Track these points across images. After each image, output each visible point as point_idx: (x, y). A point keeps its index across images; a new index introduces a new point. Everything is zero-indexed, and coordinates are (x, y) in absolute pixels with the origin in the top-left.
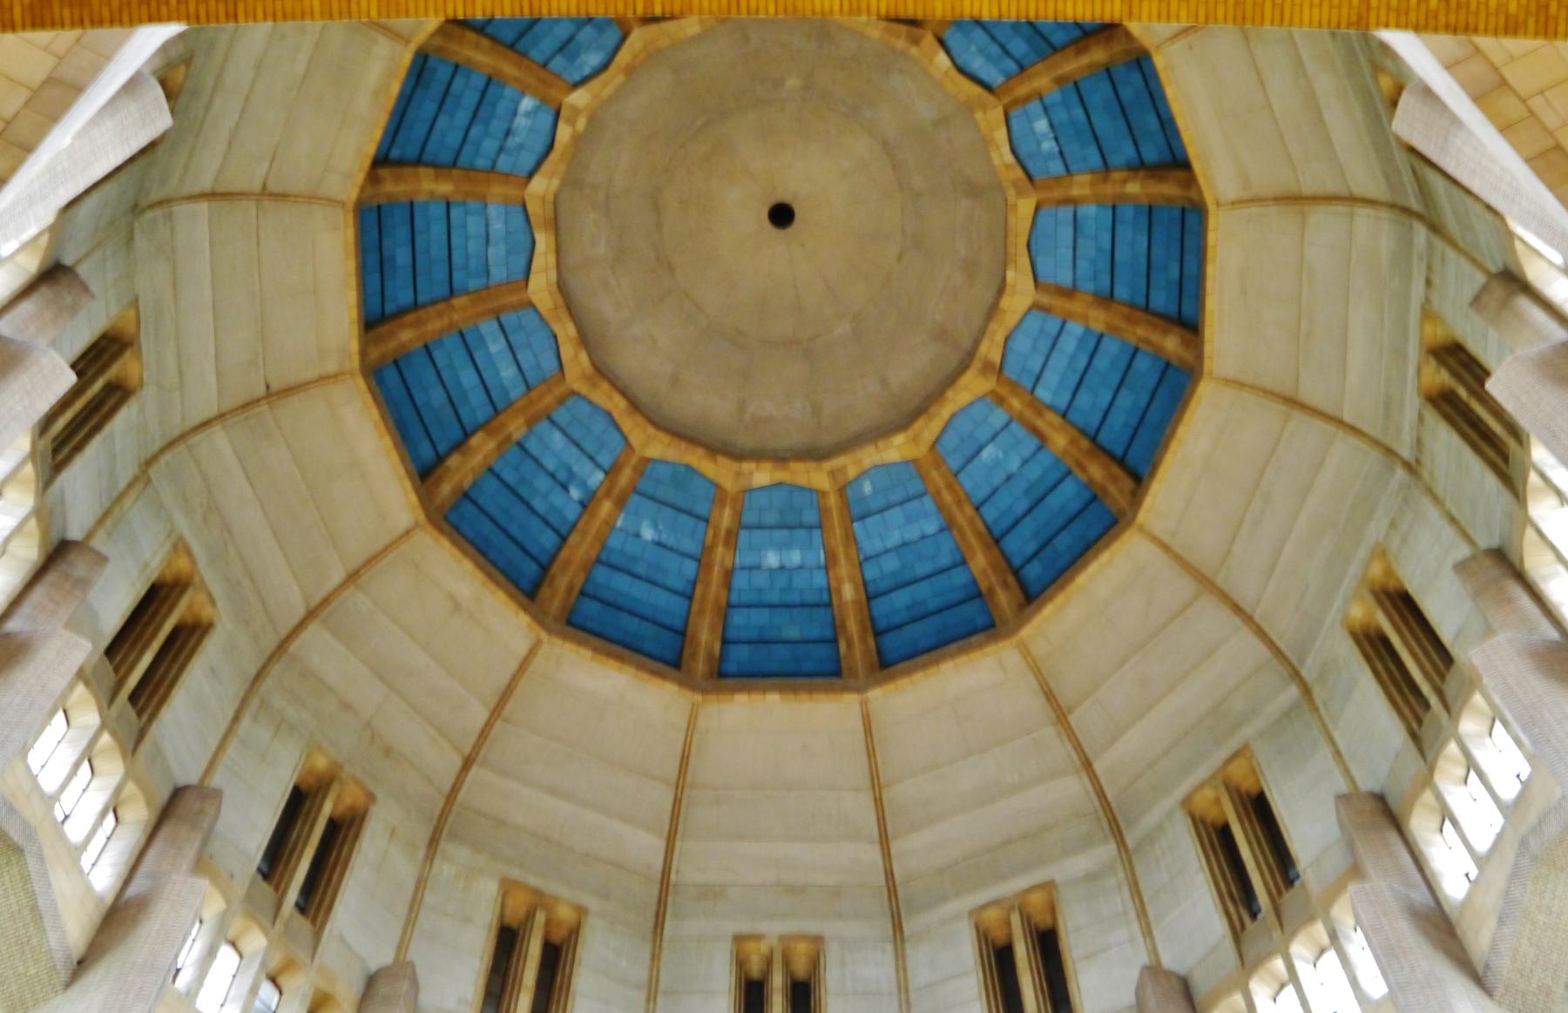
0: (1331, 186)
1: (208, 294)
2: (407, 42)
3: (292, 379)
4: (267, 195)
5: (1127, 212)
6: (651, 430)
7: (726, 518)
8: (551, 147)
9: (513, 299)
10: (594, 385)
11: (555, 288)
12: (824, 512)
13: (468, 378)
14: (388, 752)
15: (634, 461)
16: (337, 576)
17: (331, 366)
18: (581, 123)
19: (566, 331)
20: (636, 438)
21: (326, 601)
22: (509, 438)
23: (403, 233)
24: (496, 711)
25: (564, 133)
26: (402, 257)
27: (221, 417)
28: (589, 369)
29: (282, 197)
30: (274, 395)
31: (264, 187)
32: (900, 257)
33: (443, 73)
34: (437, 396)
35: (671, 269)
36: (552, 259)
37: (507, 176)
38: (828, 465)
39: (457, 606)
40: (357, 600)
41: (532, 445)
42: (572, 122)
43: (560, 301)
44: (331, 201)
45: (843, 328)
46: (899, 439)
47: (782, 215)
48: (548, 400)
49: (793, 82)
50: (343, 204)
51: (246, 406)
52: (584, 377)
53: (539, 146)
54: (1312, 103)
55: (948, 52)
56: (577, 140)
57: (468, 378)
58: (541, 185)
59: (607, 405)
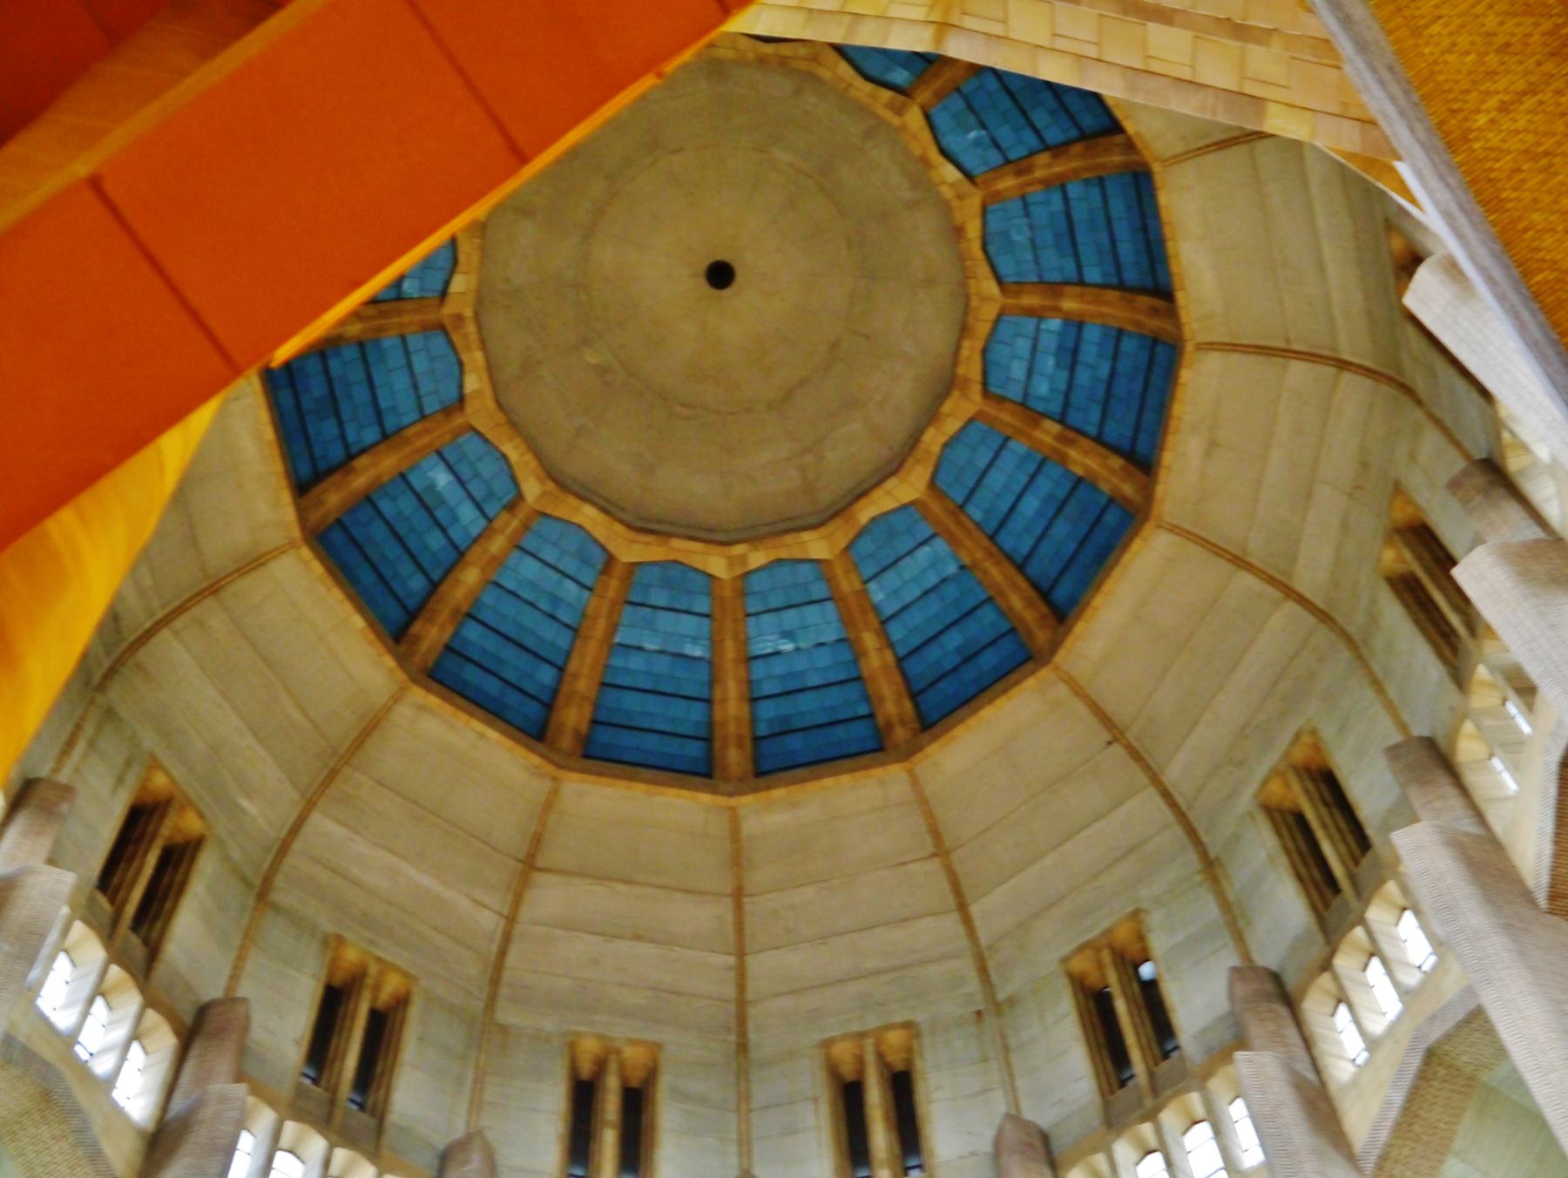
1: (1049, 860)
2: (733, 809)
3: (1092, 721)
4: (941, 851)
6: (974, 302)
7: (1007, 183)
8: (779, 561)
9: (936, 507)
10: (967, 381)
11: (902, 474)
12: (940, 96)
13: (1030, 505)
14: (1364, 466)
15: (1010, 301)
16: (1247, 580)
17: (1062, 690)
18: (739, 549)
19: (933, 440)
20: (989, 312)
21: (1272, 580)
22: (1060, 438)
23: (933, 653)
24: (1286, 353)
25: (758, 558)
26: (953, 640)
27: (1155, 779)
28: (956, 394)
29: (936, 834)
30: (1114, 731)
31: (934, 855)
32: (679, 150)
33: (768, 710)
34: (1061, 529)
35: (835, 346)
36: (877, 494)
37: (830, 581)
38: (896, 121)
39: (1212, 445)
40: (1256, 551)
41: (1056, 407)
42: (743, 559)
43: (910, 461)
44: (915, 782)
45: (782, 155)
46: (825, 73)
47: (720, 275)
48: (1006, 417)
49: (592, 359)
50: (911, 773)
51: (1135, 755)
52: (965, 395)
53: (783, 573)
55: (447, 283)
56: (754, 537)
57: (1030, 505)
59: (977, 358)
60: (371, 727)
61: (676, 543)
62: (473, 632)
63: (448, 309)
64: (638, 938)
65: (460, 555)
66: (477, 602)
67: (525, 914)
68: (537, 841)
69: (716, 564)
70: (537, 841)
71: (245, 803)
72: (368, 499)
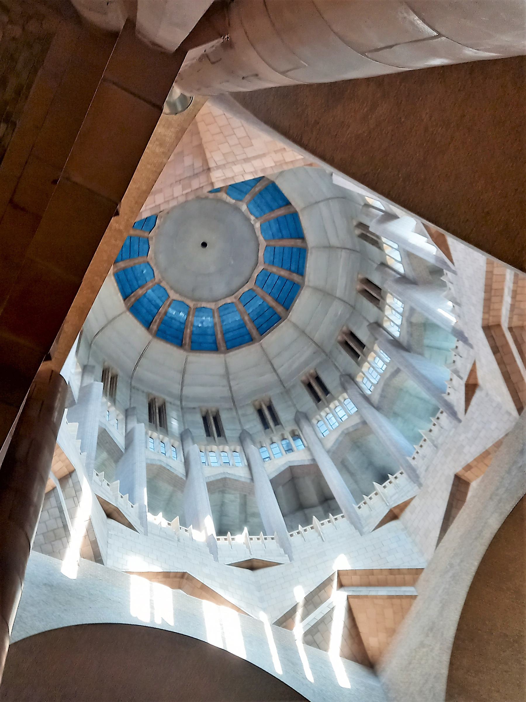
0: (186, 382)
5: (182, 326)
18: (252, 222)
25: (252, 218)
54: (203, 385)
56: (248, 220)
58: (244, 208)
60: (316, 289)
61: (257, 234)
62: (293, 268)
63: (234, 300)
64: (334, 222)
65: (280, 277)
66: (287, 270)
67: (339, 245)
68: (325, 247)
69: (257, 225)
70: (325, 247)
71: (339, 313)
72: (276, 300)
